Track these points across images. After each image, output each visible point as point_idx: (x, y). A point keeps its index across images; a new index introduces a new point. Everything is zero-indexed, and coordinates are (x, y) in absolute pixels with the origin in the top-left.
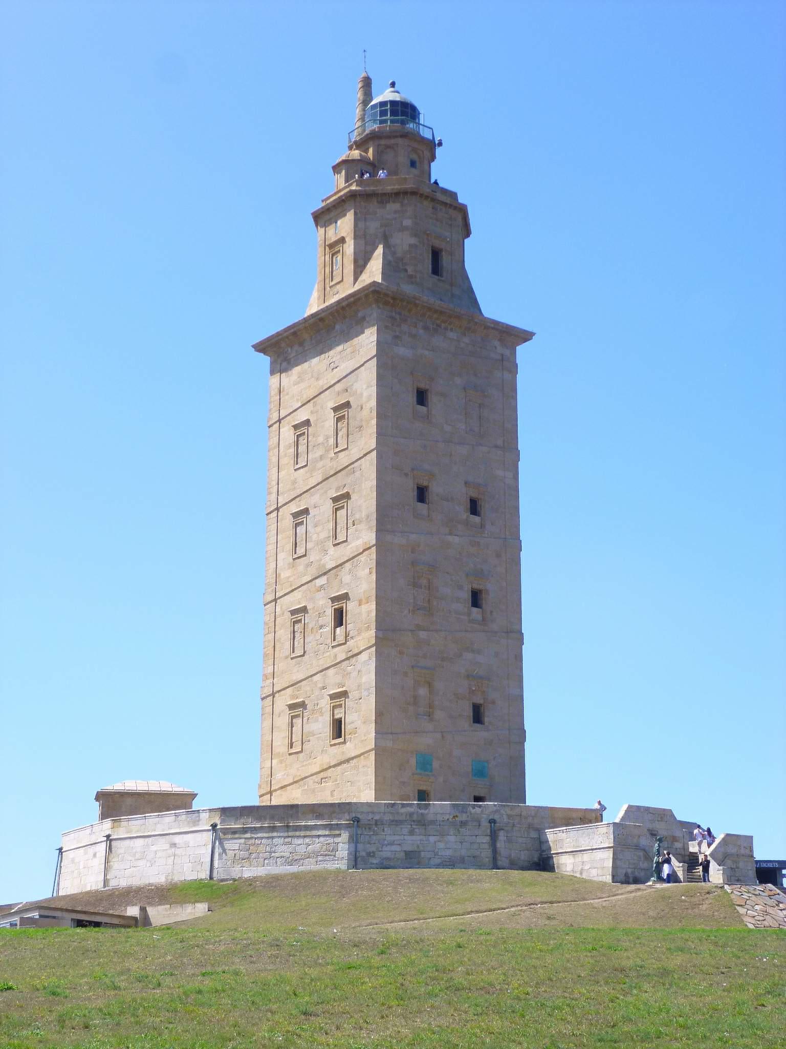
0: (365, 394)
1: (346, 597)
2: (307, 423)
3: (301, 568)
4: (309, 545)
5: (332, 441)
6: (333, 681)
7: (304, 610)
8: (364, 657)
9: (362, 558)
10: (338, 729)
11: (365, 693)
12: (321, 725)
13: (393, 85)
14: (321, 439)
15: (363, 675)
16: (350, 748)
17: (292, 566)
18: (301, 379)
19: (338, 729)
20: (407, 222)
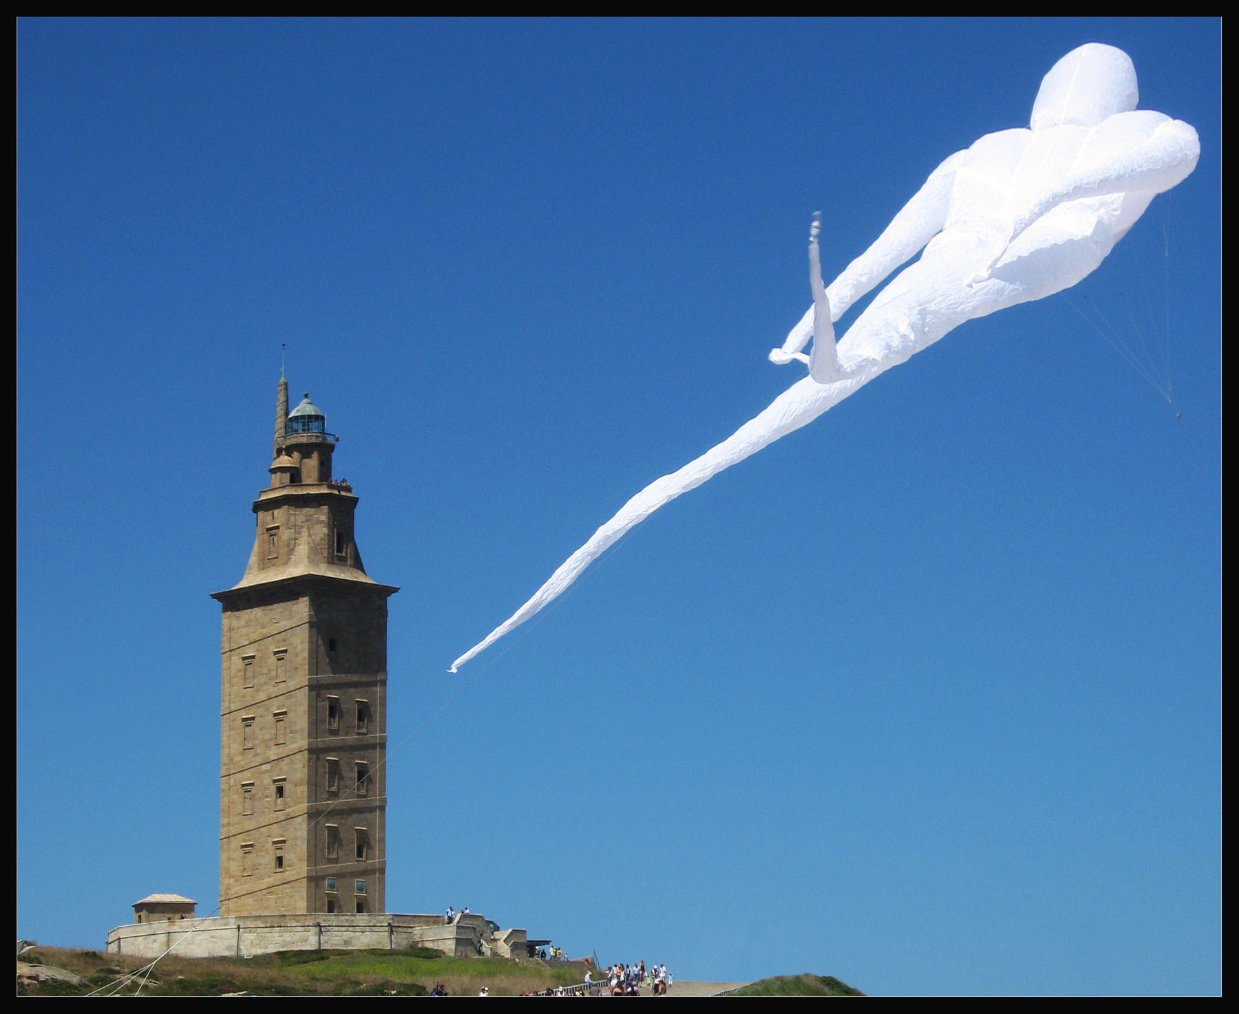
0: (299, 647)
1: (284, 780)
2: (253, 657)
3: (250, 756)
4: (257, 742)
5: (273, 674)
6: (276, 833)
7: (252, 784)
8: (299, 819)
9: (298, 756)
10: (280, 861)
11: (299, 842)
12: (269, 859)
13: (306, 396)
14: (265, 670)
15: (300, 830)
16: (289, 874)
17: (242, 754)
18: (248, 624)
19: (280, 861)
20: (324, 518)
